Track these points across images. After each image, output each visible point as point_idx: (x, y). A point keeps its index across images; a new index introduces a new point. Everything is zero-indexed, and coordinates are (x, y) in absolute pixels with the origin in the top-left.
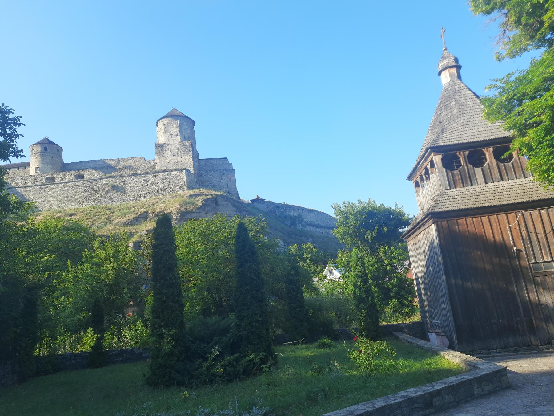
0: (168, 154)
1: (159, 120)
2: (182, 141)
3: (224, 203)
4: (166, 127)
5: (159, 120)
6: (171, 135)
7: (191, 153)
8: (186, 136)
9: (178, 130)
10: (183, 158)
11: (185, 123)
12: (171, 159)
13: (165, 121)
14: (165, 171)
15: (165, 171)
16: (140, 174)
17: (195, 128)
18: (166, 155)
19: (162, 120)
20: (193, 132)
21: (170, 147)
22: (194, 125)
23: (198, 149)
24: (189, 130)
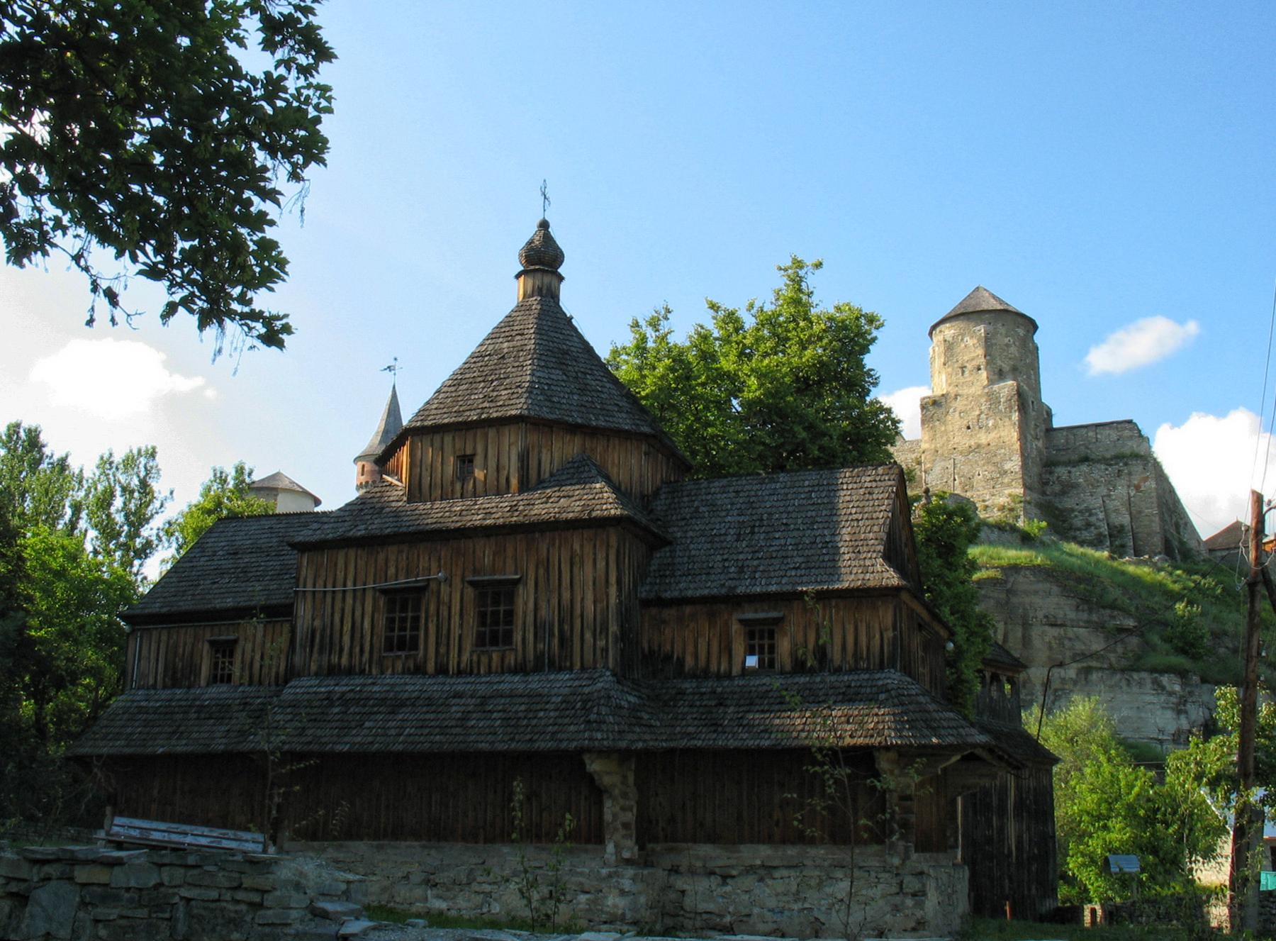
0: (954, 421)
2: (991, 382)
3: (1040, 586)
4: (949, 347)
5: (934, 327)
6: (963, 368)
7: (1015, 416)
8: (1006, 368)
9: (980, 351)
10: (993, 435)
11: (1003, 330)
12: (963, 440)
13: (948, 331)
17: (1037, 338)
19: (942, 327)
20: (1032, 352)
21: (959, 404)
22: (1035, 327)
23: (1050, 395)
24: (1013, 349)
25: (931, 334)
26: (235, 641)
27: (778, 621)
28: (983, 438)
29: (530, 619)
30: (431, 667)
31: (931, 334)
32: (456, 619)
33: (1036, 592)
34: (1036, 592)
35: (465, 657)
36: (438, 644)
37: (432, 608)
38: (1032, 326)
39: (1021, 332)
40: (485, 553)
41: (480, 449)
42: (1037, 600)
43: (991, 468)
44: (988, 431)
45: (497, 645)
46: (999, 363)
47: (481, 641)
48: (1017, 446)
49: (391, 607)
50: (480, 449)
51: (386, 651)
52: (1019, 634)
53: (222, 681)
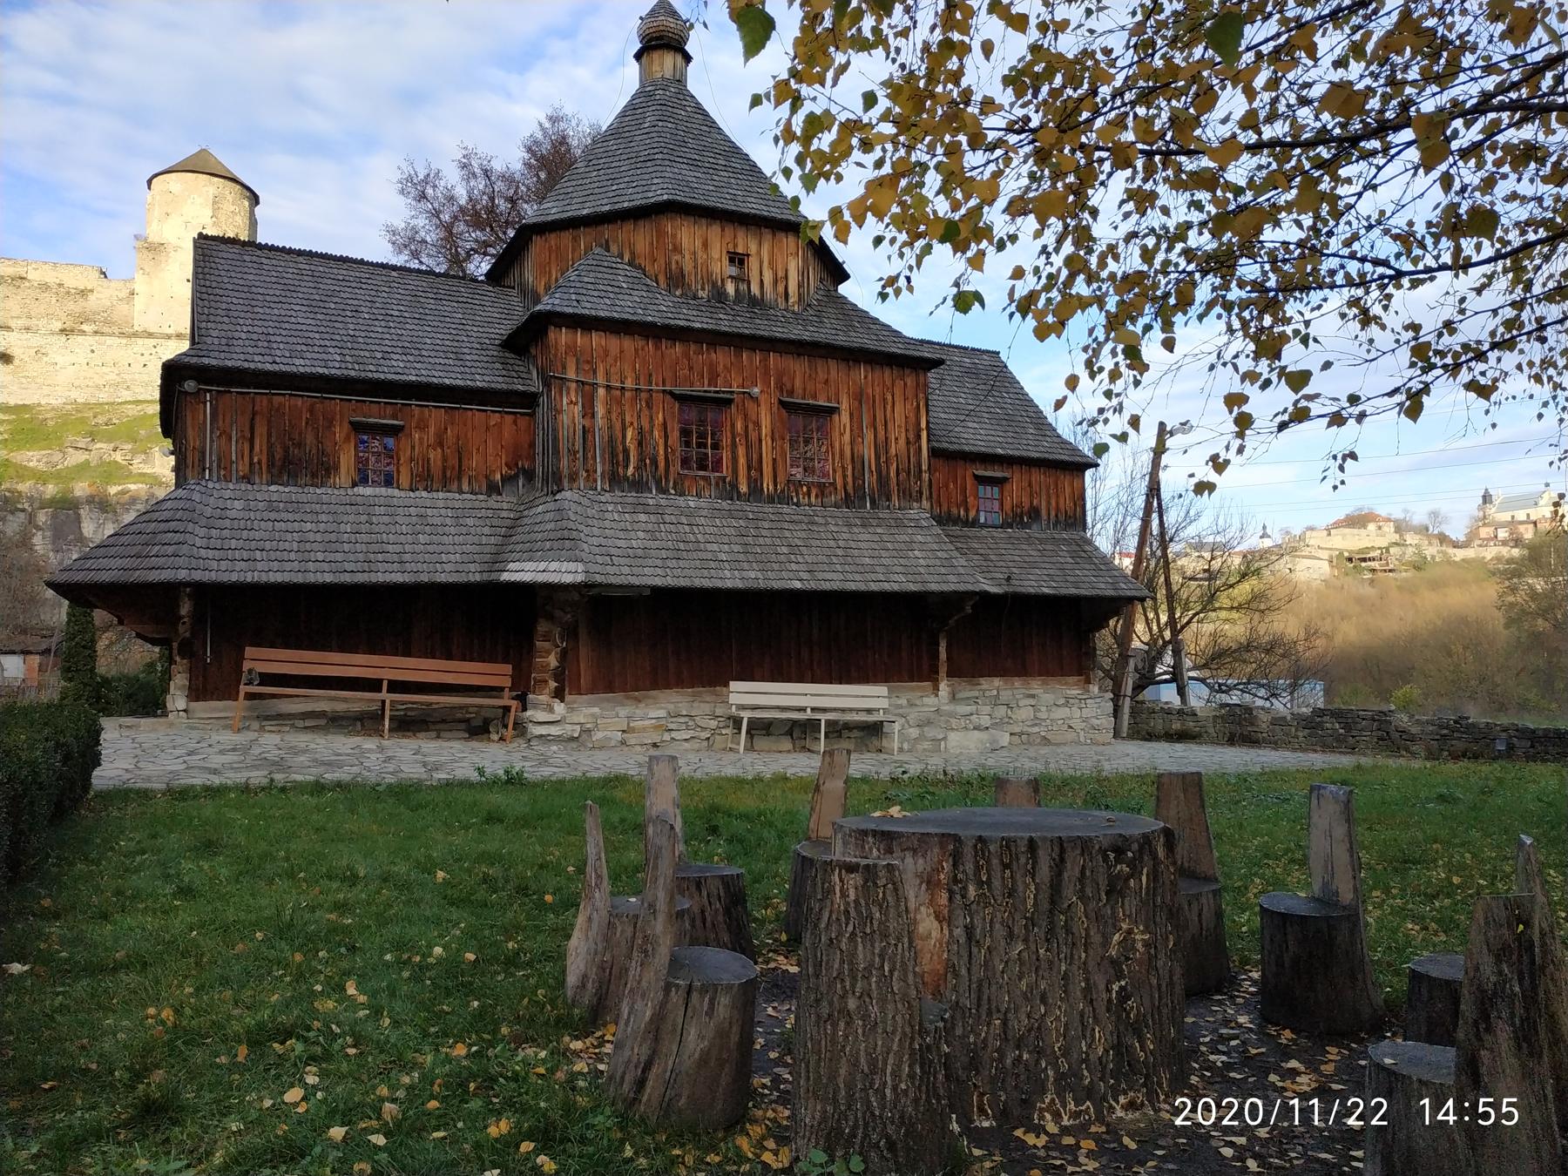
1: (156, 175)
5: (156, 175)
14: (150, 335)
15: (150, 335)
16: (83, 332)
22: (257, 203)
24: (238, 218)
25: (149, 182)
30: (744, 488)
31: (149, 182)
36: (749, 468)
37: (739, 426)
38: (255, 199)
40: (797, 369)
50: (753, 248)
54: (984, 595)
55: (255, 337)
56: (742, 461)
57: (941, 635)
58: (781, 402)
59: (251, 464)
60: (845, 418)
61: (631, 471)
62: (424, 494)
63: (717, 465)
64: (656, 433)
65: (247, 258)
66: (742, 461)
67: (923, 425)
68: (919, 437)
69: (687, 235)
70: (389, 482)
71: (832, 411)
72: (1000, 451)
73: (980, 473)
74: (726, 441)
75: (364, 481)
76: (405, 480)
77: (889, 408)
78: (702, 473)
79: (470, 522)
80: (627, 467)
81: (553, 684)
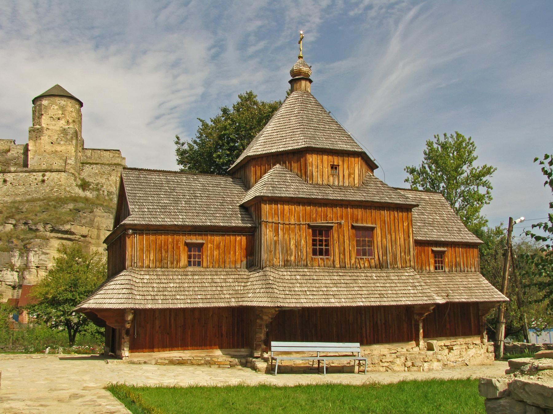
7: (74, 142)
8: (70, 121)
12: (49, 148)
18: (42, 141)
24: (74, 114)
26: (203, 244)
27: (444, 252)
28: (59, 148)
29: (379, 244)
32: (347, 241)
33: (103, 217)
34: (103, 217)
35: (353, 261)
37: (336, 236)
38: (81, 104)
39: (77, 106)
41: (341, 163)
42: (104, 220)
43: (61, 161)
44: (62, 145)
45: (365, 255)
46: (68, 118)
47: (358, 253)
48: (74, 154)
49: (314, 234)
51: (313, 255)
52: (96, 233)
53: (194, 265)
54: (438, 305)
55: (150, 210)
56: (337, 251)
57: (420, 322)
58: (353, 227)
59: (150, 260)
60: (379, 231)
61: (293, 258)
62: (212, 269)
63: (327, 253)
64: (303, 241)
65: (141, 176)
66: (337, 251)
67: (411, 231)
68: (409, 237)
69: (312, 159)
70: (199, 264)
71: (372, 229)
72: (443, 239)
73: (435, 249)
74: (331, 243)
75: (189, 264)
76: (205, 264)
77: (397, 224)
78: (321, 257)
79: (231, 280)
80: (291, 255)
81: (264, 346)
